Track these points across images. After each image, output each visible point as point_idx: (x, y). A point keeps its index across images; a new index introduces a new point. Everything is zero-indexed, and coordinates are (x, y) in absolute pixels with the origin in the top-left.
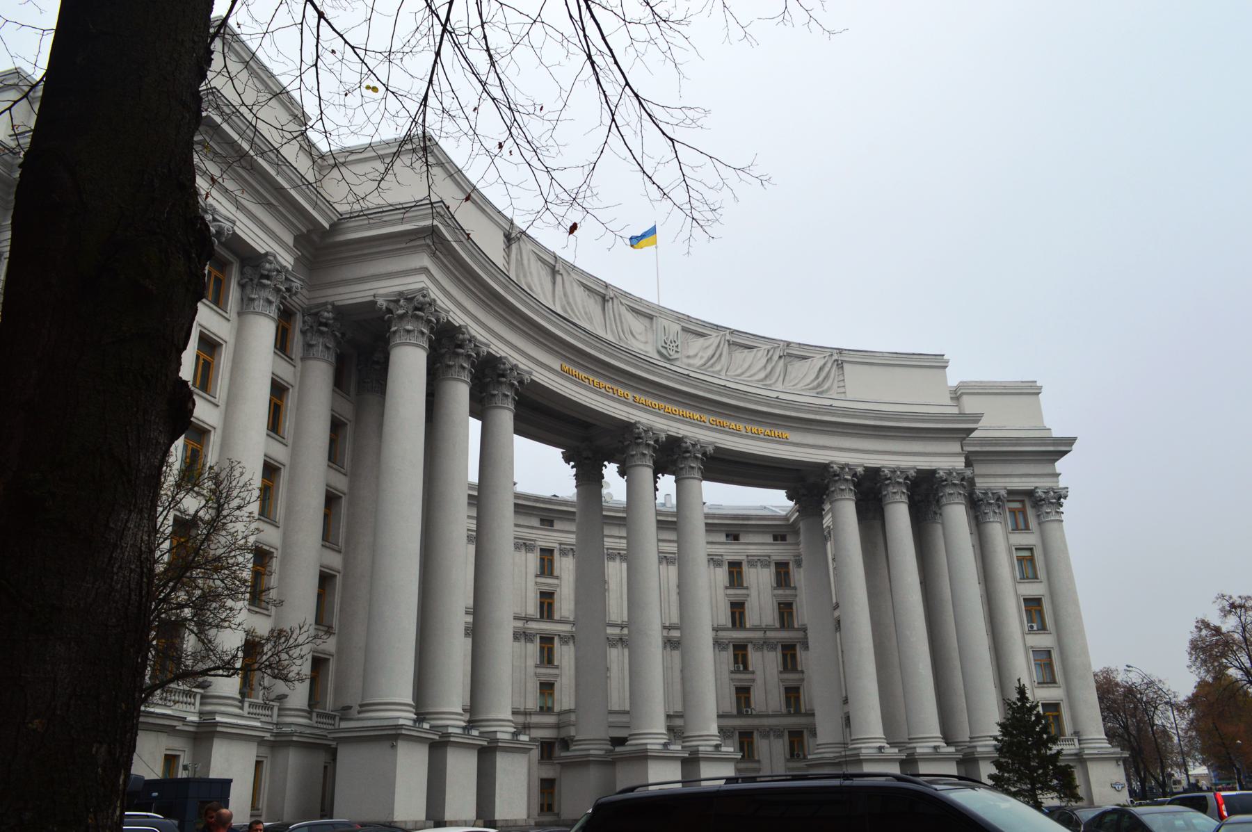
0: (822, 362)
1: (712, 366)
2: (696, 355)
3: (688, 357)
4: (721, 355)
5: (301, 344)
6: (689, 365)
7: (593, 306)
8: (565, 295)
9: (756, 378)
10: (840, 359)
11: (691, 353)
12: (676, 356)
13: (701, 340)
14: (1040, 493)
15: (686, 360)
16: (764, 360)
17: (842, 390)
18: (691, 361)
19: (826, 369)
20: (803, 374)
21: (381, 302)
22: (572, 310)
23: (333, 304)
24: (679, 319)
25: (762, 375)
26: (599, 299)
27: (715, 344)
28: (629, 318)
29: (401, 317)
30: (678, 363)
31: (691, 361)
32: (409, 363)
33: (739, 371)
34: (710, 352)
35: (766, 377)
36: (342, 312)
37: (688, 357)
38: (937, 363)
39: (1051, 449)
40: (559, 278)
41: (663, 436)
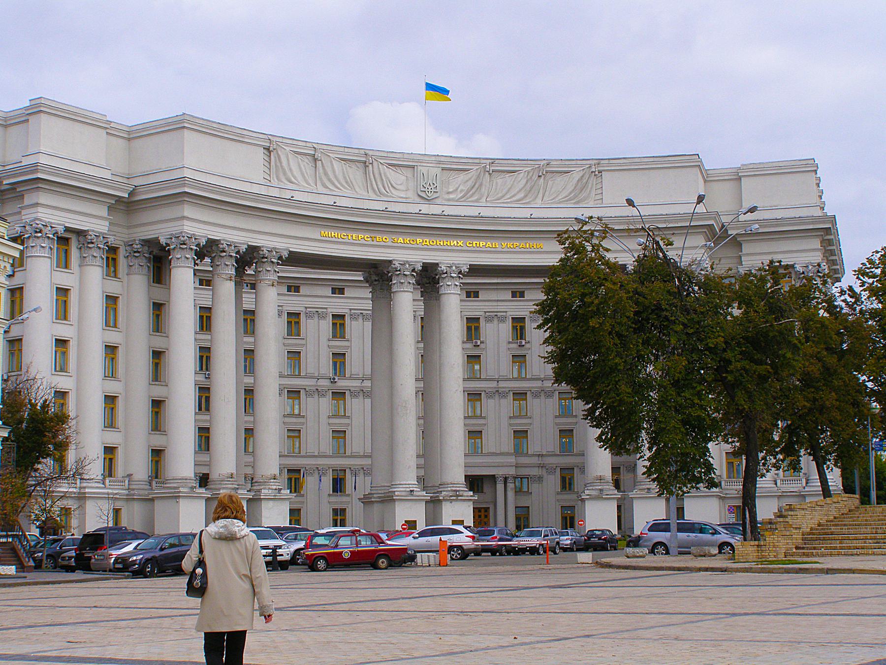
0: (581, 174)
1: (471, 196)
2: (457, 189)
3: (449, 193)
4: (481, 185)
5: (126, 264)
6: (449, 200)
7: (355, 174)
8: (326, 174)
9: (514, 199)
10: (596, 170)
11: (451, 190)
12: (435, 195)
13: (462, 176)
14: (799, 268)
15: (447, 197)
16: (524, 182)
17: (599, 197)
18: (452, 196)
19: (585, 181)
20: (561, 186)
21: (163, 241)
22: (333, 184)
23: (140, 240)
24: (440, 162)
25: (521, 195)
26: (361, 165)
27: (474, 177)
28: (391, 174)
29: (174, 249)
30: (438, 201)
31: (452, 196)
32: (183, 276)
33: (500, 195)
34: (470, 183)
35: (525, 196)
36: (147, 243)
37: (449, 193)
38: (693, 162)
39: (811, 227)
40: (319, 163)
41: (419, 267)
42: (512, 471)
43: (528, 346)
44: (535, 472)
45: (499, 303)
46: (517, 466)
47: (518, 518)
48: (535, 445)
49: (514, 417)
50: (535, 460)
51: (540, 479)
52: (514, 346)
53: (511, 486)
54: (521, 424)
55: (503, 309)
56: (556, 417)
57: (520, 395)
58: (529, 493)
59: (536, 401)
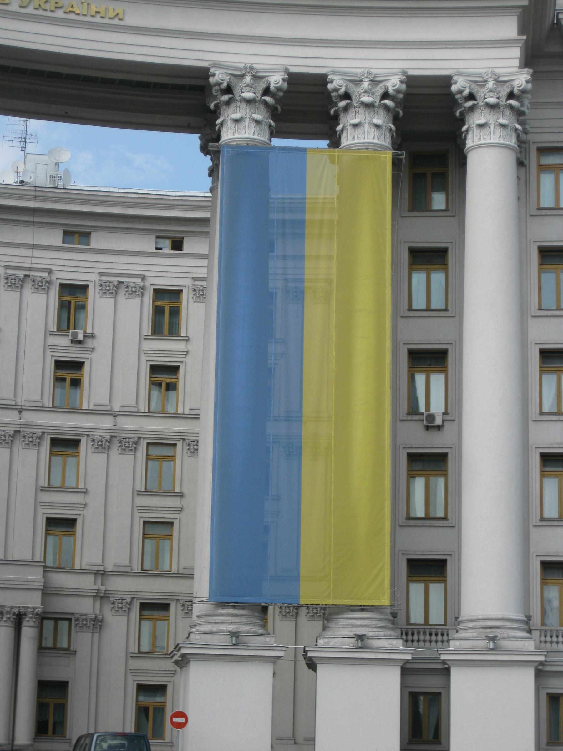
42: (34, 601)
43: (90, 343)
44: (85, 607)
45: (37, 253)
46: (47, 592)
47: (41, 708)
48: (88, 549)
49: (49, 488)
50: (87, 583)
51: (97, 624)
52: (64, 341)
53: (28, 632)
54: (61, 504)
55: (45, 263)
56: (140, 493)
57: (65, 445)
58: (69, 652)
59: (99, 459)
